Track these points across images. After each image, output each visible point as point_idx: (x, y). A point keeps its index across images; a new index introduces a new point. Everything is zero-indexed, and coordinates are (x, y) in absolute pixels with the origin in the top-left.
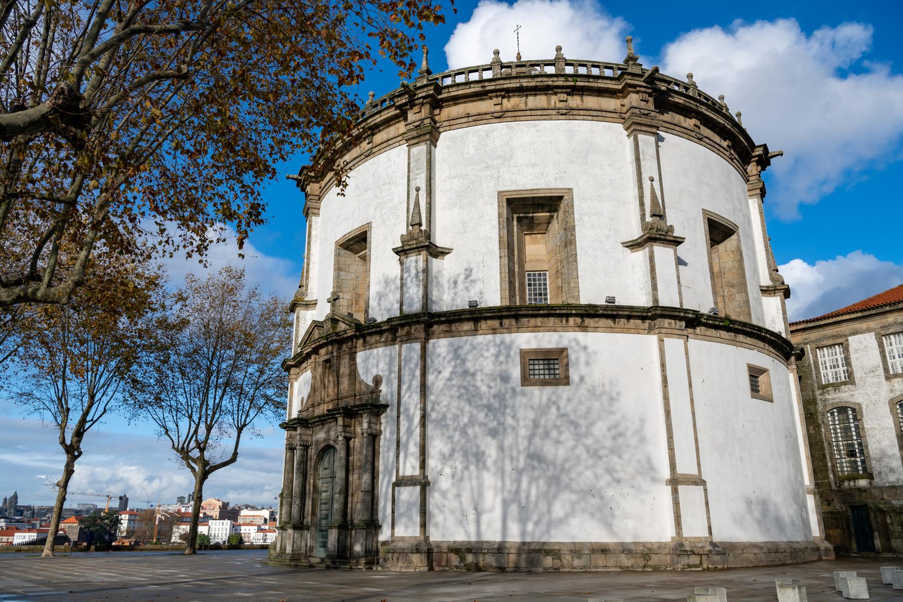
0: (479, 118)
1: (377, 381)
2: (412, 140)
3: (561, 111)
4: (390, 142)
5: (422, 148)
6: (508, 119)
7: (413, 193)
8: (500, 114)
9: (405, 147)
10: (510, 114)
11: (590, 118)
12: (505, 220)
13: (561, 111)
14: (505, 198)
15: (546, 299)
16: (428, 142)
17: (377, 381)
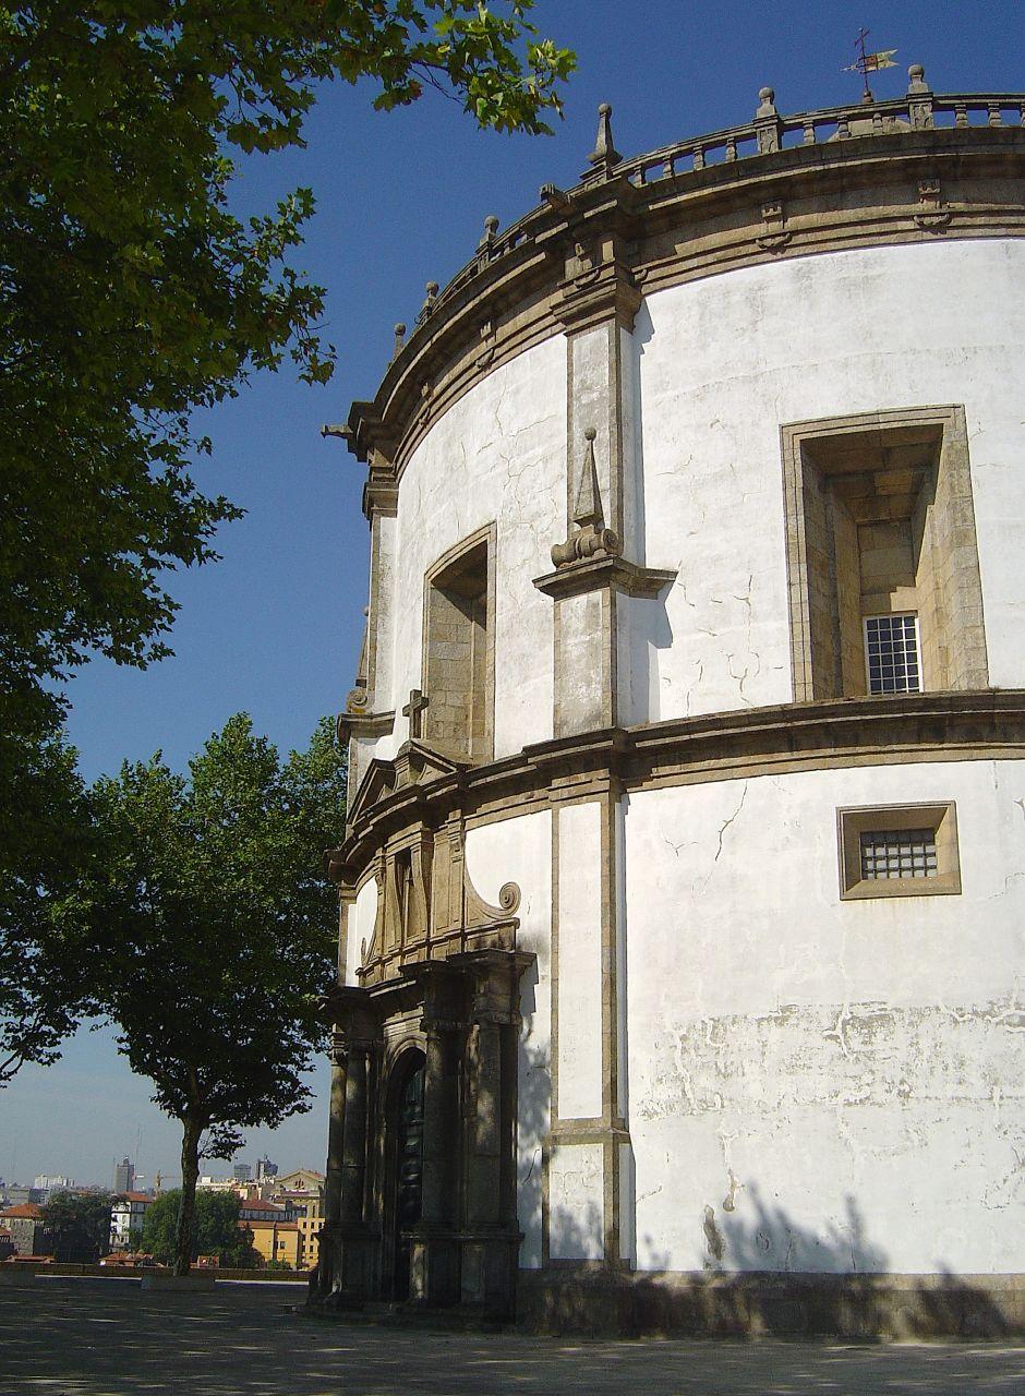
0: (730, 253)
1: (510, 897)
2: (573, 322)
3: (927, 221)
4: (533, 330)
5: (598, 338)
6: (801, 250)
7: (580, 443)
8: (779, 239)
9: (561, 339)
10: (801, 238)
11: (1002, 231)
12: (800, 494)
13: (927, 221)
14: (798, 438)
15: (914, 682)
16: (612, 322)
17: (510, 897)
